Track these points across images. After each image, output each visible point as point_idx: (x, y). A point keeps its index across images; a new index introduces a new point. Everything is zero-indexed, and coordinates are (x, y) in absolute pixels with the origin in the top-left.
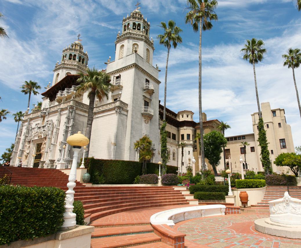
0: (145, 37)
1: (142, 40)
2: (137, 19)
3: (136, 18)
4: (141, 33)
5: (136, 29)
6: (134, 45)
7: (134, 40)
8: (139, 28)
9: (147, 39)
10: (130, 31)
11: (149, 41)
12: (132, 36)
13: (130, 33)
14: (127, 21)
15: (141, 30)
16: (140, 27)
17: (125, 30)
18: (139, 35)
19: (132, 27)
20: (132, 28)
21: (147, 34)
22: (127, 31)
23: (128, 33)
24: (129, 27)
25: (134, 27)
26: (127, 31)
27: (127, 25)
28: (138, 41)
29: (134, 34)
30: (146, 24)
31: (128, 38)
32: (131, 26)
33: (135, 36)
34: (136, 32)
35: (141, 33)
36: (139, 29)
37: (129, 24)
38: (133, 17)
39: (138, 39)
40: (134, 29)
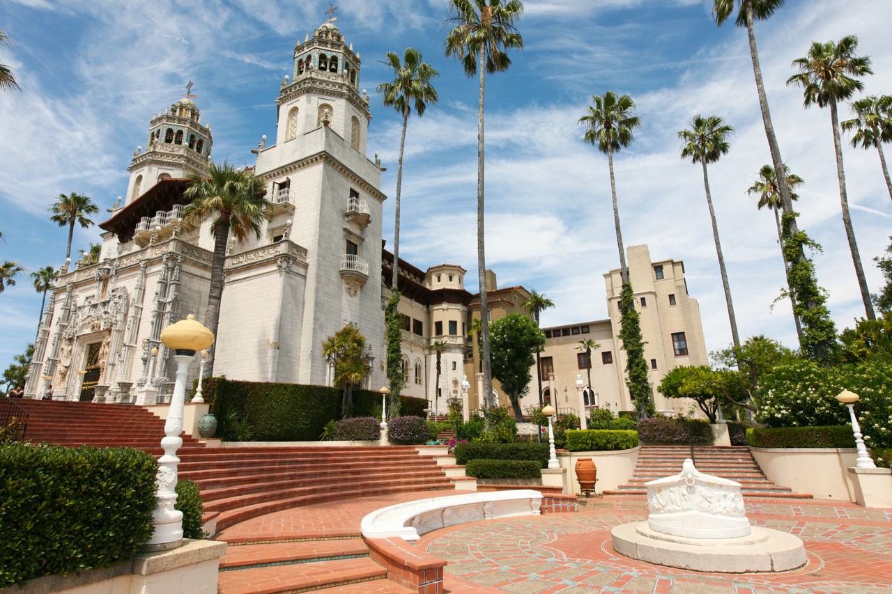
0: (349, 90)
1: (341, 95)
2: (329, 46)
3: (327, 43)
4: (338, 78)
5: (328, 70)
6: (322, 107)
7: (321, 96)
8: (333, 67)
9: (354, 94)
10: (314, 75)
11: (358, 97)
12: (317, 85)
13: (311, 78)
14: (306, 50)
15: (339, 72)
16: (336, 65)
17: (301, 72)
18: (334, 84)
19: (317, 64)
20: (317, 68)
21: (352, 81)
22: (305, 75)
23: (307, 79)
24: (311, 64)
25: (323, 65)
26: (305, 75)
27: (304, 60)
28: (332, 98)
29: (322, 82)
30: (351, 58)
31: (308, 91)
32: (314, 63)
33: (324, 86)
34: (326, 76)
35: (338, 78)
36: (334, 71)
37: (309, 58)
38: (320, 42)
39: (332, 93)
40: (321, 69)
